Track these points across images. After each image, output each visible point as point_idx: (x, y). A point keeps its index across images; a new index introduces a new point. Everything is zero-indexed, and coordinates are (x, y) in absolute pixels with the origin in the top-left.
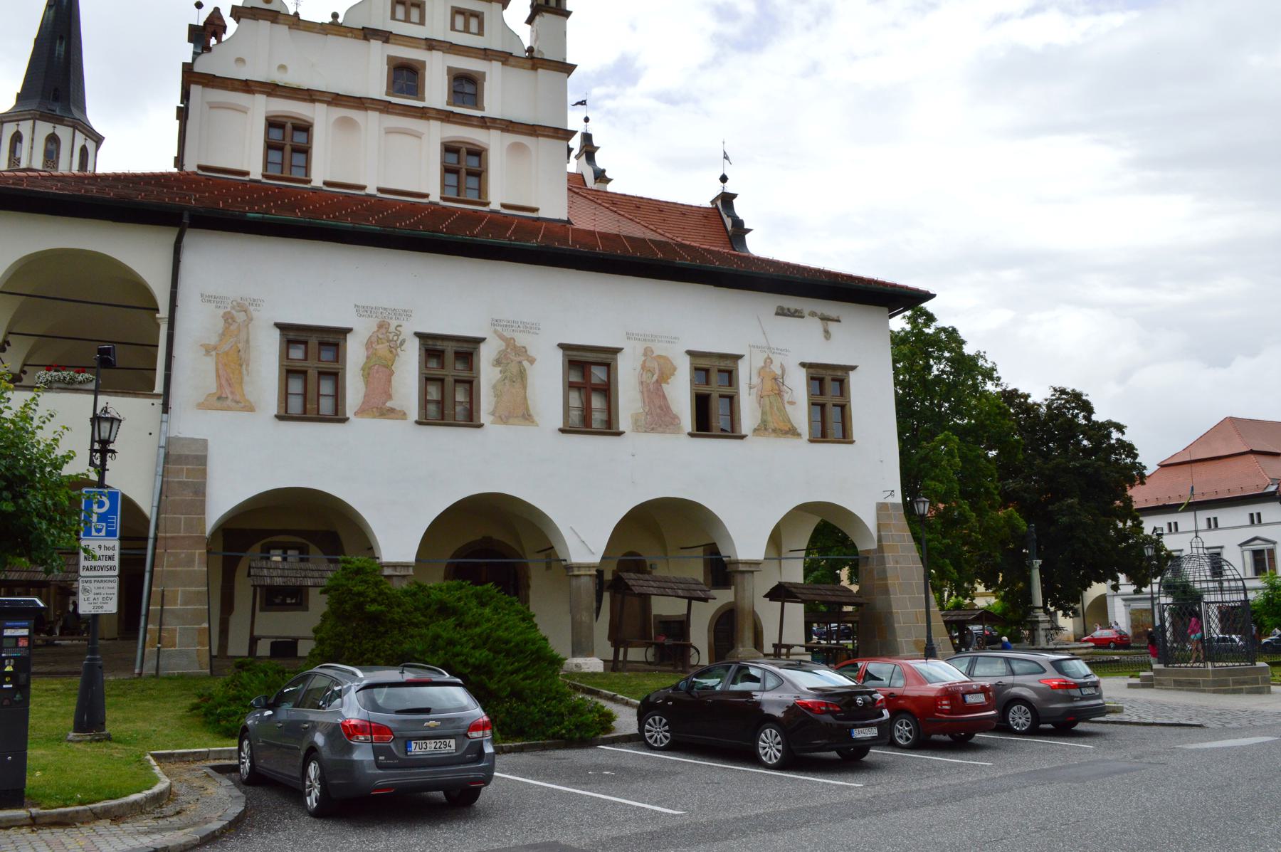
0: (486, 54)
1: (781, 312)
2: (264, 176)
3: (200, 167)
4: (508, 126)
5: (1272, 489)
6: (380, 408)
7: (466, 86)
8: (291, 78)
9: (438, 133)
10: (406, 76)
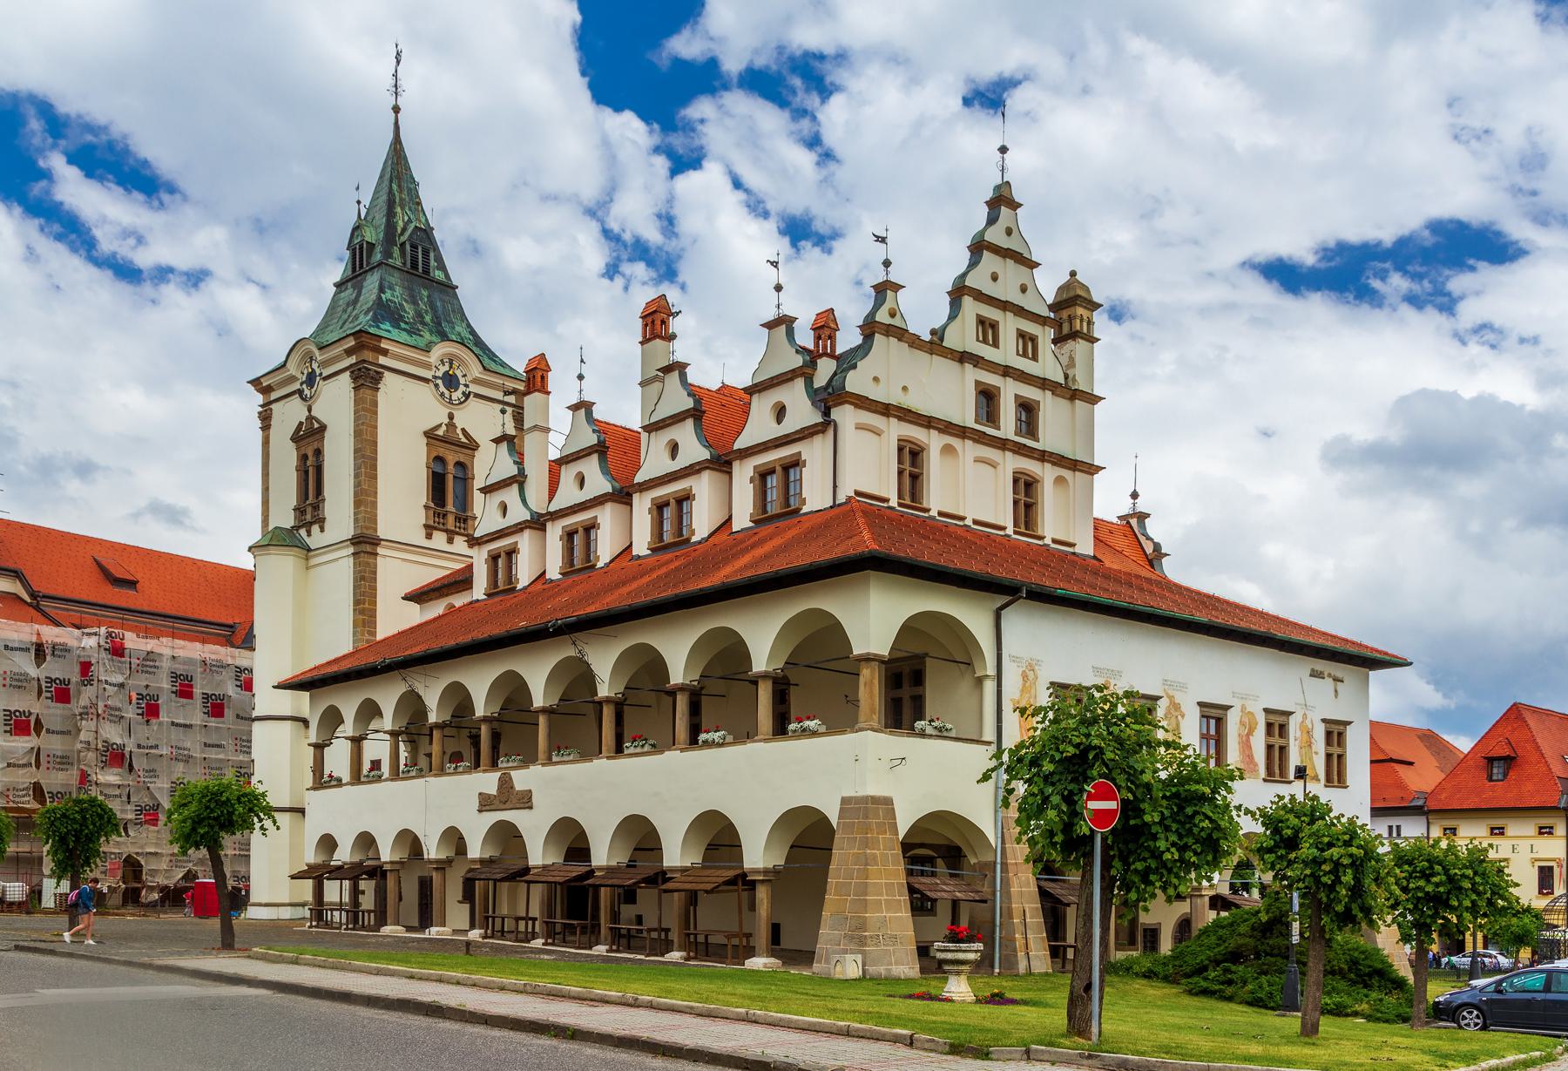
0: (1043, 383)
1: (1315, 674)
2: (900, 505)
3: (858, 493)
5: (1420, 803)
8: (912, 402)
9: (1011, 463)
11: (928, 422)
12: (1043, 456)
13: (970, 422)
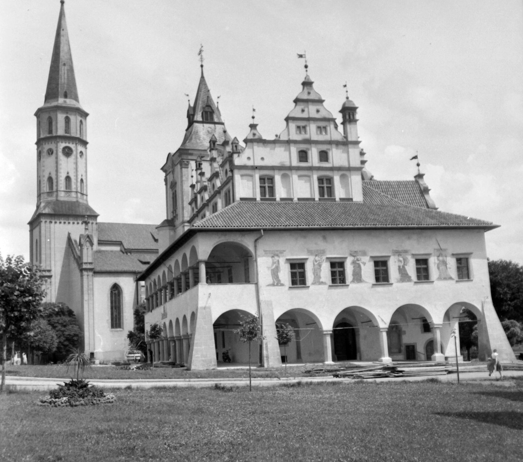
0: (330, 142)
4: (339, 169)
6: (317, 281)
7: (324, 156)
10: (303, 156)
11: (273, 168)
12: (332, 169)
13: (295, 162)
